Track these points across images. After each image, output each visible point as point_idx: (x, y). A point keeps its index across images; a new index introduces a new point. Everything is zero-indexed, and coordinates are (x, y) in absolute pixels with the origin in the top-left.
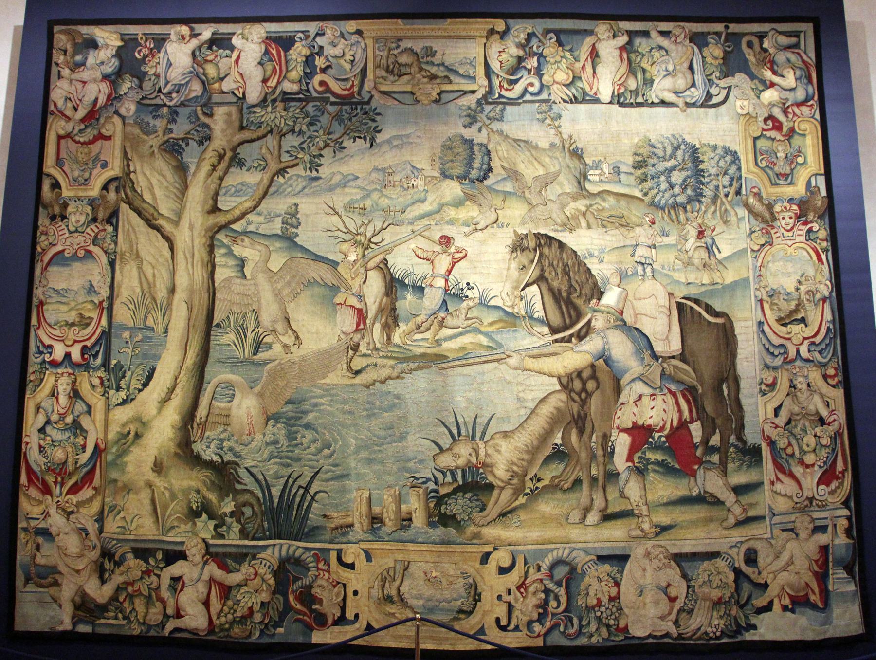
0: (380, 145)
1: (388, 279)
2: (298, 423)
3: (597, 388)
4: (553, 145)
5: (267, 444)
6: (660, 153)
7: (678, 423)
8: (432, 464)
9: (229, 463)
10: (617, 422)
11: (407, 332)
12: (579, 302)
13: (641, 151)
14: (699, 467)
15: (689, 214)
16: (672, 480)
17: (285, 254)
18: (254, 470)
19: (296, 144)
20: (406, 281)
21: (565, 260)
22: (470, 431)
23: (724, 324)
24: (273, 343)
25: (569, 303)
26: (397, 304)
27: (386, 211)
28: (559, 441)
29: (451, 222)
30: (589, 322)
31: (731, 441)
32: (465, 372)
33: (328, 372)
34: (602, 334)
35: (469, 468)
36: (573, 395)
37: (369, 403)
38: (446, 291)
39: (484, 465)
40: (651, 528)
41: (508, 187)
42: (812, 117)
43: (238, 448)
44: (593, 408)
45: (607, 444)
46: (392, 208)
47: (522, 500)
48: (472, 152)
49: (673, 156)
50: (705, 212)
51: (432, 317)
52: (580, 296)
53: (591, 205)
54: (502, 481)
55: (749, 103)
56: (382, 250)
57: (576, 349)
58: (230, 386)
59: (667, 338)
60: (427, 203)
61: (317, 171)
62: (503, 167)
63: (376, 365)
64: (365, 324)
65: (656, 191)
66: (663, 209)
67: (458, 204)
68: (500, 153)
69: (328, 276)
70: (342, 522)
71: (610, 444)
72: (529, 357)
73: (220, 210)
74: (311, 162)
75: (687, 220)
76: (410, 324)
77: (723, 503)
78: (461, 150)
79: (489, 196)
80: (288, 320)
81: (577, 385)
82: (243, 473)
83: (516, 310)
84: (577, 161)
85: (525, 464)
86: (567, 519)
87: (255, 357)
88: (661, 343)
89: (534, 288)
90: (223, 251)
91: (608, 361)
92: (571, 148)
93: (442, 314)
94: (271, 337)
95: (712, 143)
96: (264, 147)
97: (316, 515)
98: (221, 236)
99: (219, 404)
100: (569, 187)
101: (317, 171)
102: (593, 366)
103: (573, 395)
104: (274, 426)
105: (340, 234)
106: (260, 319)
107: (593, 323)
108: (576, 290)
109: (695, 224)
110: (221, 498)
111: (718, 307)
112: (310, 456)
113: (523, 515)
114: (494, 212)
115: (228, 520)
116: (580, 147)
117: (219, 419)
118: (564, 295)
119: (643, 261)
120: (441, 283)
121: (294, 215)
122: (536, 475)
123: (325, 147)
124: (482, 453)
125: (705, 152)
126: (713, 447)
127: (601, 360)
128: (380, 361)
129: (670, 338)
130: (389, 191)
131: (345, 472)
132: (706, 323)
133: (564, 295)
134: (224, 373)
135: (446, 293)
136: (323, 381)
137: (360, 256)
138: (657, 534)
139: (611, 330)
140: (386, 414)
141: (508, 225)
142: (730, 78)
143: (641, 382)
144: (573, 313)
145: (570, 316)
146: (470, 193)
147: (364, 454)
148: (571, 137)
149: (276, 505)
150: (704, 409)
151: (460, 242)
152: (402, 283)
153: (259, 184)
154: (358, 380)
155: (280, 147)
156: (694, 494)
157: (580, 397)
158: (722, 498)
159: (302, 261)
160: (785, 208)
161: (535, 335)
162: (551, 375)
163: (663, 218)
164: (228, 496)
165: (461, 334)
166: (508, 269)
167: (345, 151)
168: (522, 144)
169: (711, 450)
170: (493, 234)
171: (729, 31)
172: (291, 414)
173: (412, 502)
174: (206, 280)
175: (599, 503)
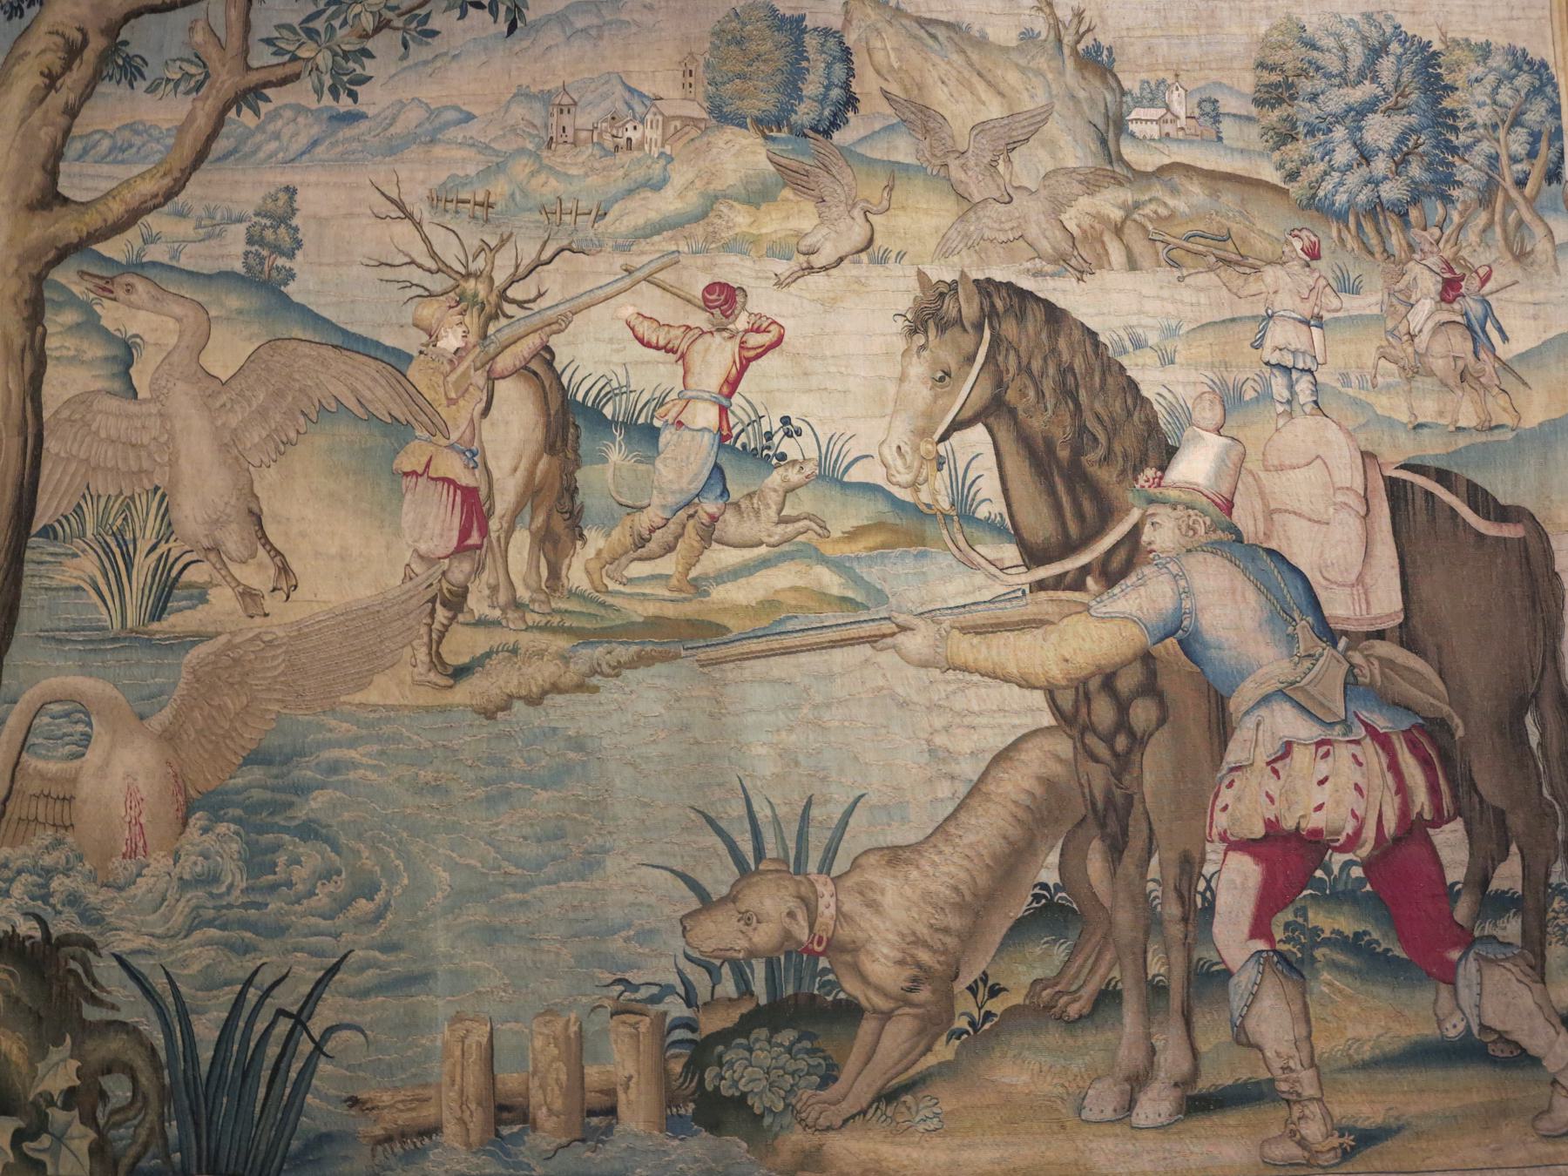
0: (536, 27)
1: (555, 405)
2: (279, 819)
3: (1162, 721)
4: (1028, 36)
5: (184, 885)
6: (1335, 66)
7: (1399, 826)
8: (679, 943)
9: (65, 940)
10: (1221, 821)
11: (605, 555)
12: (1106, 476)
13: (1278, 57)
14: (1465, 955)
15: (1416, 233)
16: (1384, 992)
17: (255, 328)
18: (140, 963)
19: (295, 20)
20: (608, 411)
21: (1066, 357)
22: (792, 845)
23: (1522, 541)
24: (211, 584)
25: (1077, 476)
26: (579, 475)
27: (552, 212)
28: (1050, 876)
29: (741, 245)
30: (1136, 531)
31: (1554, 880)
32: (776, 673)
33: (372, 672)
34: (1174, 568)
35: (788, 954)
36: (1091, 740)
37: (493, 761)
38: (723, 438)
39: (834, 947)
40: (1328, 1135)
41: (903, 150)
43: (94, 897)
44: (1149, 779)
45: (1192, 885)
46: (568, 205)
47: (944, 1051)
48: (800, 52)
49: (1369, 72)
50: (1461, 227)
51: (682, 514)
52: (1107, 459)
53: (1137, 205)
54: (886, 995)
56: (536, 320)
57: (1099, 609)
58: (79, 709)
59: (1360, 579)
60: (669, 192)
61: (353, 95)
62: (886, 94)
63: (514, 651)
64: (484, 531)
65: (1322, 166)
66: (1341, 217)
67: (757, 196)
68: (879, 57)
69: (380, 393)
70: (403, 1118)
71: (1202, 886)
72: (964, 630)
73: (65, 201)
74: (336, 72)
75: (1411, 248)
76: (616, 534)
77: (1535, 1061)
78: (769, 45)
79: (847, 173)
80: (257, 518)
81: (1103, 712)
82: (106, 970)
83: (925, 497)
84: (1098, 83)
85: (951, 942)
86: (1079, 1110)
87: (155, 626)
88: (1342, 595)
89: (978, 433)
90: (70, 317)
91: (1191, 643)
92: (1081, 47)
93: (710, 506)
94: (205, 566)
95: (1476, 38)
96: (201, 24)
97: (326, 1098)
98: (65, 276)
99: (41, 764)
100: (1076, 153)
101: (353, 95)
102: (1146, 658)
103: (1091, 740)
104: (205, 830)
105: (416, 275)
106: (174, 515)
107: (1147, 535)
108: (1096, 440)
109: (1432, 261)
110: (39, 1050)
111: (1505, 494)
112: (313, 920)
113: (947, 1098)
114: (860, 219)
115: (57, 1116)
116: (1105, 41)
117: (41, 809)
118: (1064, 454)
119: (1288, 360)
120: (706, 416)
121: (283, 219)
122: (985, 977)
123: (377, 30)
124: (827, 911)
125: (1459, 64)
126: (1501, 895)
127: (1171, 642)
128: (526, 640)
129: (1368, 580)
130: (559, 157)
131: (416, 968)
132: (1472, 539)
133: (1064, 454)
134: (59, 671)
135: (721, 445)
136: (358, 697)
137: (472, 339)
138: (1346, 1154)
139: (1200, 556)
140: (544, 795)
141: (901, 256)
143: (1287, 706)
144: (1088, 506)
145: (1080, 516)
146: (794, 165)
147: (476, 913)
148: (1079, 15)
149: (204, 1068)
150: (1473, 786)
151: (762, 300)
152: (594, 415)
153: (181, 130)
154: (462, 694)
155: (247, 26)
156: (1452, 1033)
157: (1112, 748)
158: (1535, 1045)
159: (304, 349)
161: (978, 567)
162: (1026, 684)
163: (1342, 240)
164: (58, 1042)
165: (765, 563)
166: (902, 378)
167: (435, 41)
168: (941, 33)
169: (1496, 905)
170: (858, 281)
172: (257, 794)
173: (617, 1057)
174: (15, 403)
175: (1172, 1059)
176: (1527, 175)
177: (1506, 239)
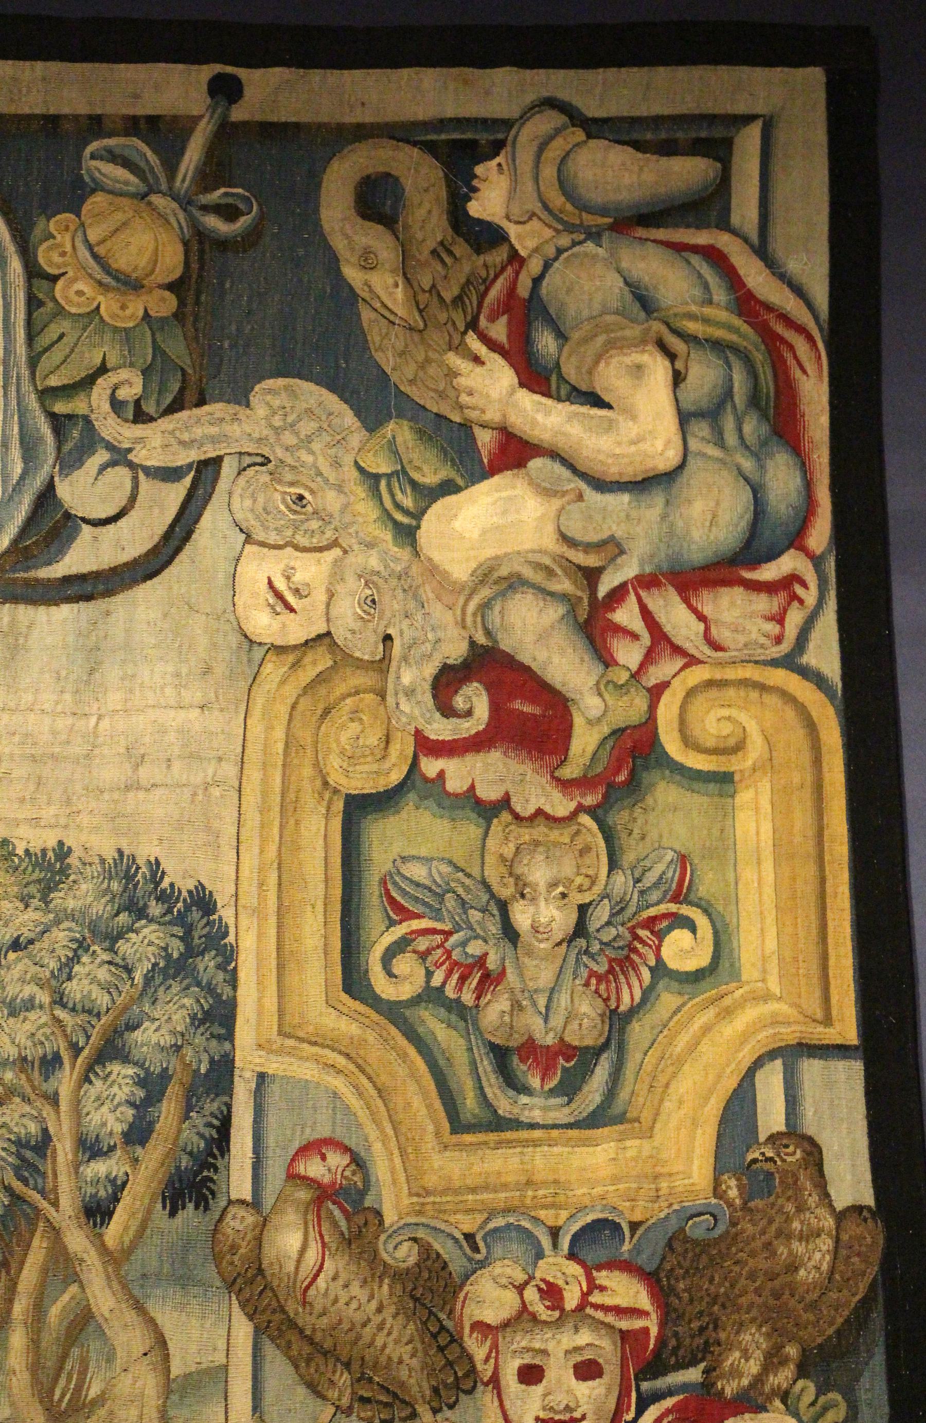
42: (789, 662)
55: (337, 573)
142: (216, 409)
160: (551, 1293)
171: (238, 114)
176: (118, 1188)
177: (35, 1368)
